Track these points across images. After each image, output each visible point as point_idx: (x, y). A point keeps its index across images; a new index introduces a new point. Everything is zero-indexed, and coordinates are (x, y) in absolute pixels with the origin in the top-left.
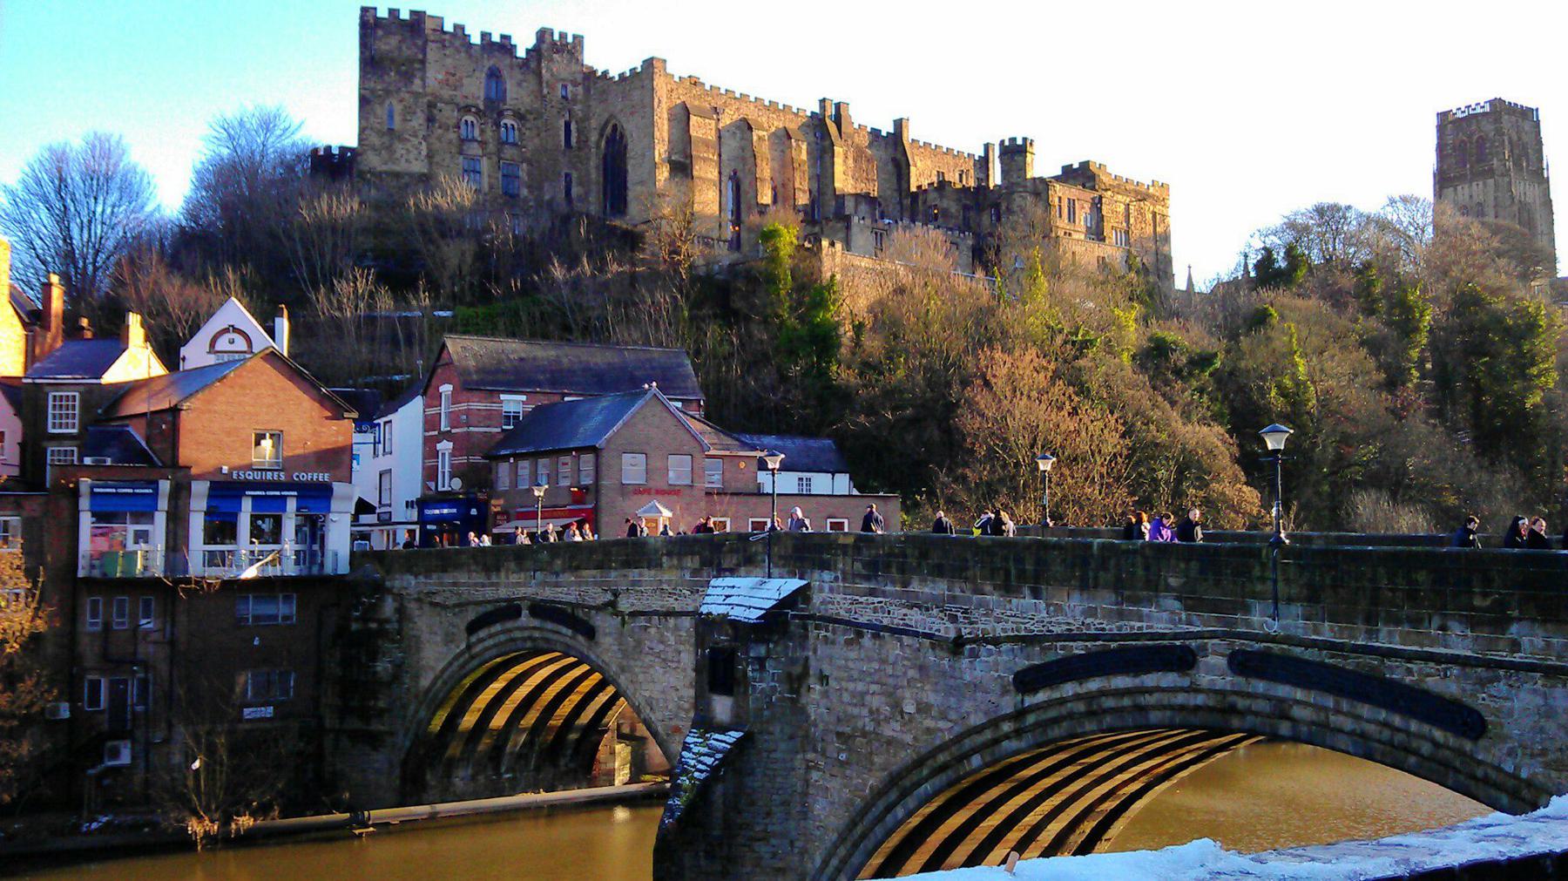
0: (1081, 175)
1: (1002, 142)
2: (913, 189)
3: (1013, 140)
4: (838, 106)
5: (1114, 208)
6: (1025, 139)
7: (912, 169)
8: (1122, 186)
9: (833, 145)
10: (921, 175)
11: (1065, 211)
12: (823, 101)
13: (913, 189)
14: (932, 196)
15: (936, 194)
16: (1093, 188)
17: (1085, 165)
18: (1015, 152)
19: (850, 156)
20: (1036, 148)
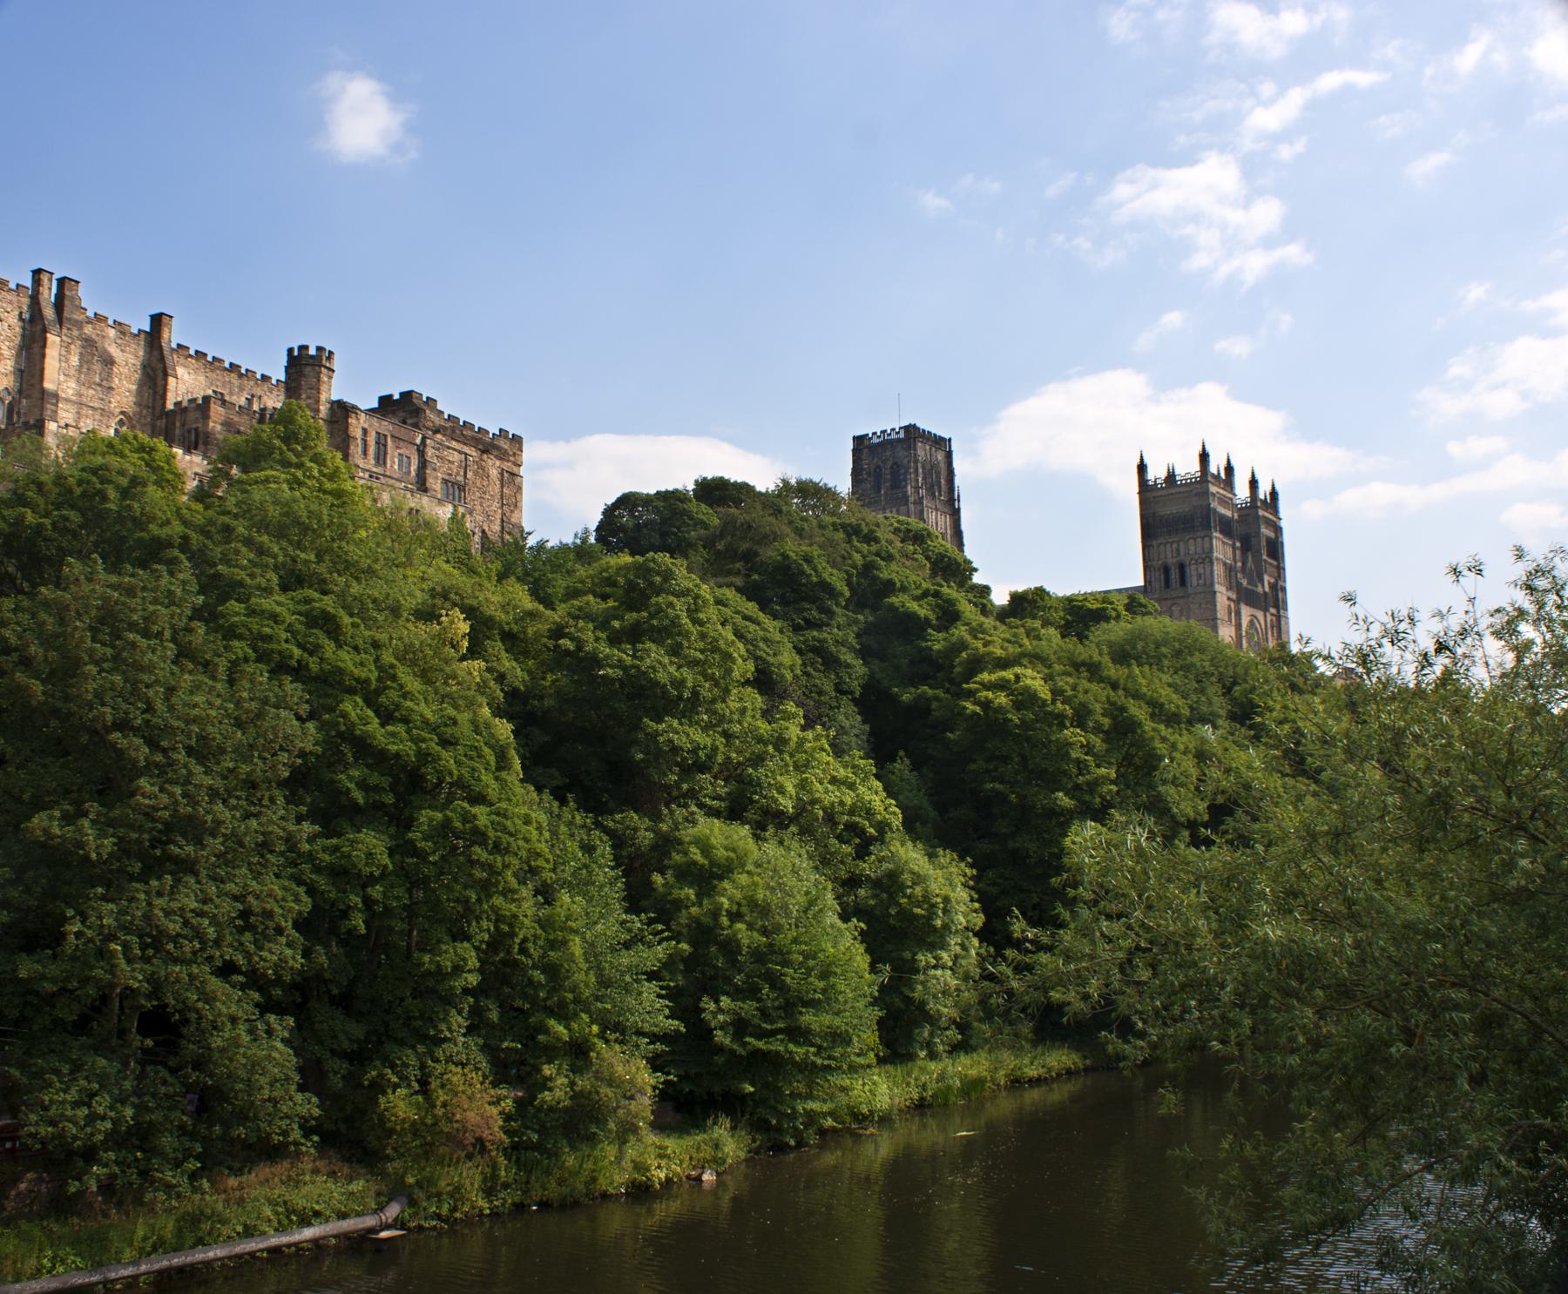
0: (403, 409)
1: (290, 351)
2: (170, 406)
3: (303, 348)
4: (62, 282)
5: (448, 458)
6: (320, 349)
7: (171, 380)
8: (457, 430)
9: (45, 331)
10: (185, 384)
11: (372, 450)
12: (37, 273)
13: (170, 406)
14: (192, 416)
15: (198, 414)
16: (416, 425)
17: (407, 396)
18: (305, 366)
19: (75, 349)
20: (336, 364)
